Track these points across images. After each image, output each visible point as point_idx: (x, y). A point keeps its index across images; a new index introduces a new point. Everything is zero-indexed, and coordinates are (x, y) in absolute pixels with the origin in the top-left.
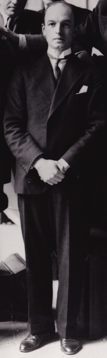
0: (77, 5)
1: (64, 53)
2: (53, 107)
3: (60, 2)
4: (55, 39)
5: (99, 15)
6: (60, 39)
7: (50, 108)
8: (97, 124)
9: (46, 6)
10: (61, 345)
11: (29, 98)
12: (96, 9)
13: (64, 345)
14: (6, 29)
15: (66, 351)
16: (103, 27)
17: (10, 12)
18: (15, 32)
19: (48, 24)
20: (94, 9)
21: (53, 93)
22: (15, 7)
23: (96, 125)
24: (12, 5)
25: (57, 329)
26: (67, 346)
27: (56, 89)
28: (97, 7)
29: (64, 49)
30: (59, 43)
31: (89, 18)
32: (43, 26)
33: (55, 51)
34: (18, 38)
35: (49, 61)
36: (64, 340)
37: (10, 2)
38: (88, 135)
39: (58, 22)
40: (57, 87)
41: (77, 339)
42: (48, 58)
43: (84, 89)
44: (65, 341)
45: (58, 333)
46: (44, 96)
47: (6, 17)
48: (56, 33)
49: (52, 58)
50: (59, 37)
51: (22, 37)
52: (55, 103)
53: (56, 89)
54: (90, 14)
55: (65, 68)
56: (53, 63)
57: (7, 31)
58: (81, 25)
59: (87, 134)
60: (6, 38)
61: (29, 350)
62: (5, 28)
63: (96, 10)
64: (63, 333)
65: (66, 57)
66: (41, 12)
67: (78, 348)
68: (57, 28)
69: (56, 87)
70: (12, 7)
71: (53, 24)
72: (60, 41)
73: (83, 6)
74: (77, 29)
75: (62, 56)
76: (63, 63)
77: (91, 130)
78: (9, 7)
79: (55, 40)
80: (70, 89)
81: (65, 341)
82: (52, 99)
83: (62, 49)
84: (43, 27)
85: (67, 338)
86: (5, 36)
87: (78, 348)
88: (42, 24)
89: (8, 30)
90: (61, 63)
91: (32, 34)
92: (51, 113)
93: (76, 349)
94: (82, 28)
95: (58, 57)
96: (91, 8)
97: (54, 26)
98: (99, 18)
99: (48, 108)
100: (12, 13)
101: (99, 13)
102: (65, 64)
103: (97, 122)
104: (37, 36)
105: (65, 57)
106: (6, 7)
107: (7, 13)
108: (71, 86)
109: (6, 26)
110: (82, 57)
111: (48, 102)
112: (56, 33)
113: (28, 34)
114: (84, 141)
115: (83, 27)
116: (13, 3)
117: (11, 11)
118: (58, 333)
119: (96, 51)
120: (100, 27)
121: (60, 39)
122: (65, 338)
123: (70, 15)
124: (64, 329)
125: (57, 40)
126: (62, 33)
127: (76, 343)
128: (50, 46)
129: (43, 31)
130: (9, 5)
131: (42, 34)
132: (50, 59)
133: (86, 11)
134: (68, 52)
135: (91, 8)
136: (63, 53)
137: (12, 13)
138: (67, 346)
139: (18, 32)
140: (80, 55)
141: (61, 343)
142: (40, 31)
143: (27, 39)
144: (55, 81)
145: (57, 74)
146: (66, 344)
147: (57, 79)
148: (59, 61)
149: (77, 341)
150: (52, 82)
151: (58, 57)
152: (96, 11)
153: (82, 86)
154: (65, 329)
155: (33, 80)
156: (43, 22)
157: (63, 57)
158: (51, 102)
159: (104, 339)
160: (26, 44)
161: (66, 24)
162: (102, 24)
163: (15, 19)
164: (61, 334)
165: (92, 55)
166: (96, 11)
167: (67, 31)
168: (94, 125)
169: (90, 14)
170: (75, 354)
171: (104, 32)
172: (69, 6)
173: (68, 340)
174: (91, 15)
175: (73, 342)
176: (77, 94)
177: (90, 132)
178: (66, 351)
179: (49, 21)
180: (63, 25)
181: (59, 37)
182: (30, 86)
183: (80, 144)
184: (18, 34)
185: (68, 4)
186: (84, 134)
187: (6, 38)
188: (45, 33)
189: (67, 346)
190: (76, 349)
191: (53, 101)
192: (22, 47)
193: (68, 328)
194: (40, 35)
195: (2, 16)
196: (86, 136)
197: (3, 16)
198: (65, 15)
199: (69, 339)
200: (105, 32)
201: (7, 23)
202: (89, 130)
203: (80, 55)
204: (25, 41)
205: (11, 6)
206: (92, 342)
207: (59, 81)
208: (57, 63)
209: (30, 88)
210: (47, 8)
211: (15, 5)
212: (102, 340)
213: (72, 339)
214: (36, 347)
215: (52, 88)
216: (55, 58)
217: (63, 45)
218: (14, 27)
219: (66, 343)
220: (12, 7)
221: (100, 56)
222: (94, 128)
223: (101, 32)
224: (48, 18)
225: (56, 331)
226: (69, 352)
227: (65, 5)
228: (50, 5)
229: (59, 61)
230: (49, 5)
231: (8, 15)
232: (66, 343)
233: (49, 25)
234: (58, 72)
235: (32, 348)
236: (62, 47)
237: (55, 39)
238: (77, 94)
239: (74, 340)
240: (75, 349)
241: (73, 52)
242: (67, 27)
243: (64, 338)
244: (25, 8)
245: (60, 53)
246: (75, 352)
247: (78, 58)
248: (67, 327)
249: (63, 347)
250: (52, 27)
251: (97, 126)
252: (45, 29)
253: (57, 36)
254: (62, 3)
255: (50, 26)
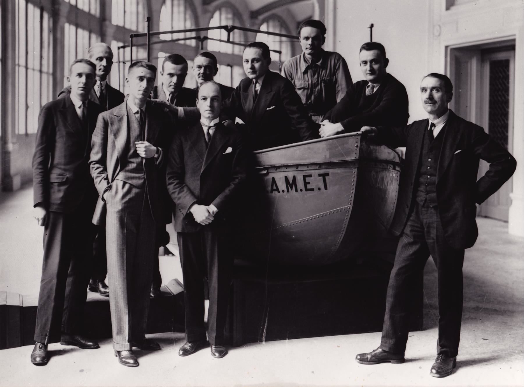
0: (224, 84)
1: (214, 122)
2: (205, 164)
3: (211, 82)
4: (206, 111)
5: (241, 92)
6: (210, 111)
7: (202, 165)
8: (239, 177)
9: (199, 85)
10: (212, 351)
11: (186, 157)
12: (238, 87)
13: (214, 351)
14: (168, 103)
15: (215, 355)
16: (244, 101)
17: (171, 89)
18: (175, 105)
19: (202, 98)
20: (237, 87)
21: (205, 153)
22: (175, 85)
23: (239, 178)
24: (172, 84)
25: (208, 338)
26: (215, 352)
27: (207, 150)
28: (240, 85)
29: (213, 118)
30: (210, 113)
31: (233, 95)
32: (197, 100)
33: (207, 120)
34: (177, 110)
35: (202, 128)
36: (214, 346)
37: (171, 82)
38: (232, 186)
39: (209, 97)
40: (208, 148)
41: (224, 346)
42: (201, 126)
43: (229, 150)
44: (214, 347)
45: (208, 341)
46: (198, 155)
47: (168, 93)
48: (207, 106)
49: (204, 126)
50: (210, 109)
51: (180, 109)
52: (206, 161)
53: (207, 150)
54: (234, 91)
55: (215, 133)
56: (205, 129)
57: (169, 104)
58: (227, 100)
59: (231, 185)
60: (168, 110)
61: (186, 354)
62: (167, 102)
63: (239, 88)
64: (213, 341)
65: (215, 125)
66: (196, 90)
67: (224, 353)
68: (208, 102)
69: (207, 149)
70: (173, 86)
71: (205, 99)
72: (210, 112)
73: (229, 85)
74: (223, 103)
75: (212, 124)
76: (213, 129)
77: (235, 182)
78: (171, 86)
79: (206, 112)
80: (218, 150)
81: (214, 347)
82: (204, 157)
83: (212, 118)
84: (197, 101)
85: (216, 345)
86: (167, 108)
87: (224, 353)
88: (197, 99)
89: (170, 104)
90: (211, 129)
91: (188, 107)
92: (204, 169)
93: (223, 354)
94: (227, 102)
95: (209, 125)
96: (235, 87)
97: (206, 101)
98: (241, 94)
99: (201, 165)
100: (173, 90)
101: (241, 91)
102: (214, 130)
103: (240, 176)
104: (192, 108)
105: (214, 124)
106: (168, 86)
107: (168, 91)
108: (219, 148)
109: (168, 101)
110: (227, 125)
111: (201, 160)
112: (207, 106)
113: (185, 107)
114: (229, 190)
115: (228, 101)
116: (174, 83)
117: (172, 89)
118: (208, 341)
119: (238, 120)
120: (242, 101)
121: (210, 111)
122: (214, 344)
123: (217, 91)
124: (214, 338)
125: (81, 89)
126: (212, 106)
127: (223, 349)
128: (203, 116)
129: (197, 105)
130: (170, 84)
131: (196, 106)
132: (203, 126)
133: (231, 89)
134: (217, 121)
135: (235, 87)
136: (213, 121)
137: (173, 90)
138: (215, 352)
139: (177, 105)
140: (226, 123)
141: (211, 349)
142: (194, 104)
143: (184, 110)
144: (207, 144)
145: (208, 138)
146: (216, 350)
147: (208, 142)
148: (210, 127)
149: (223, 347)
150: (204, 144)
151: (209, 125)
152: (238, 89)
153: (228, 148)
154: (215, 338)
155: (189, 143)
156: (197, 97)
157: (213, 125)
158: (204, 160)
159: (245, 346)
160: (183, 114)
161: (215, 99)
162: (243, 99)
163: (175, 95)
164: (211, 342)
165: (236, 123)
166: (238, 89)
167: (216, 104)
168: (237, 178)
169: (234, 91)
170: (222, 358)
171: (245, 105)
172: (218, 85)
173: (217, 346)
174: (235, 92)
175: (220, 348)
176: (224, 153)
177: (234, 184)
178: (215, 355)
179: (202, 96)
180: (213, 99)
181: (210, 109)
182: (187, 147)
183: (226, 193)
184: (178, 106)
185: (217, 83)
186: (229, 185)
187: (168, 110)
188: (198, 106)
189: (216, 351)
190: (223, 354)
191: (205, 159)
192: (180, 117)
193: (217, 337)
194: (195, 108)
195: (165, 92)
196: (231, 186)
197: (165, 92)
198: (214, 92)
199: (217, 345)
200: (246, 105)
201: (169, 98)
202: (233, 182)
203: (226, 123)
204: (183, 112)
205: (172, 85)
206: (236, 349)
207: (209, 144)
208: (208, 130)
209: (186, 149)
210: (200, 86)
211: (175, 84)
212: (244, 346)
213: (220, 346)
214: (191, 352)
215: (204, 149)
216: (207, 126)
217: (213, 115)
218: (174, 101)
219: (215, 349)
220: (173, 86)
221: (242, 124)
222: (237, 180)
223: (243, 105)
224: (201, 94)
225: (207, 339)
226: (217, 356)
227: (214, 84)
228: (202, 84)
229: (210, 127)
230: (201, 84)
231: (170, 92)
232: (215, 349)
233: (202, 99)
234: (208, 136)
235: (188, 353)
236: (212, 117)
237: (206, 111)
238: (224, 153)
239: (221, 347)
240: (222, 354)
241: (221, 121)
242: (216, 101)
243: (213, 345)
244: (183, 86)
245: (211, 122)
246: (222, 356)
247: (225, 125)
248: (216, 336)
249: (213, 352)
250: (204, 101)
251: (240, 178)
252: (199, 103)
253: (208, 108)
254: (212, 82)
255: (203, 100)
